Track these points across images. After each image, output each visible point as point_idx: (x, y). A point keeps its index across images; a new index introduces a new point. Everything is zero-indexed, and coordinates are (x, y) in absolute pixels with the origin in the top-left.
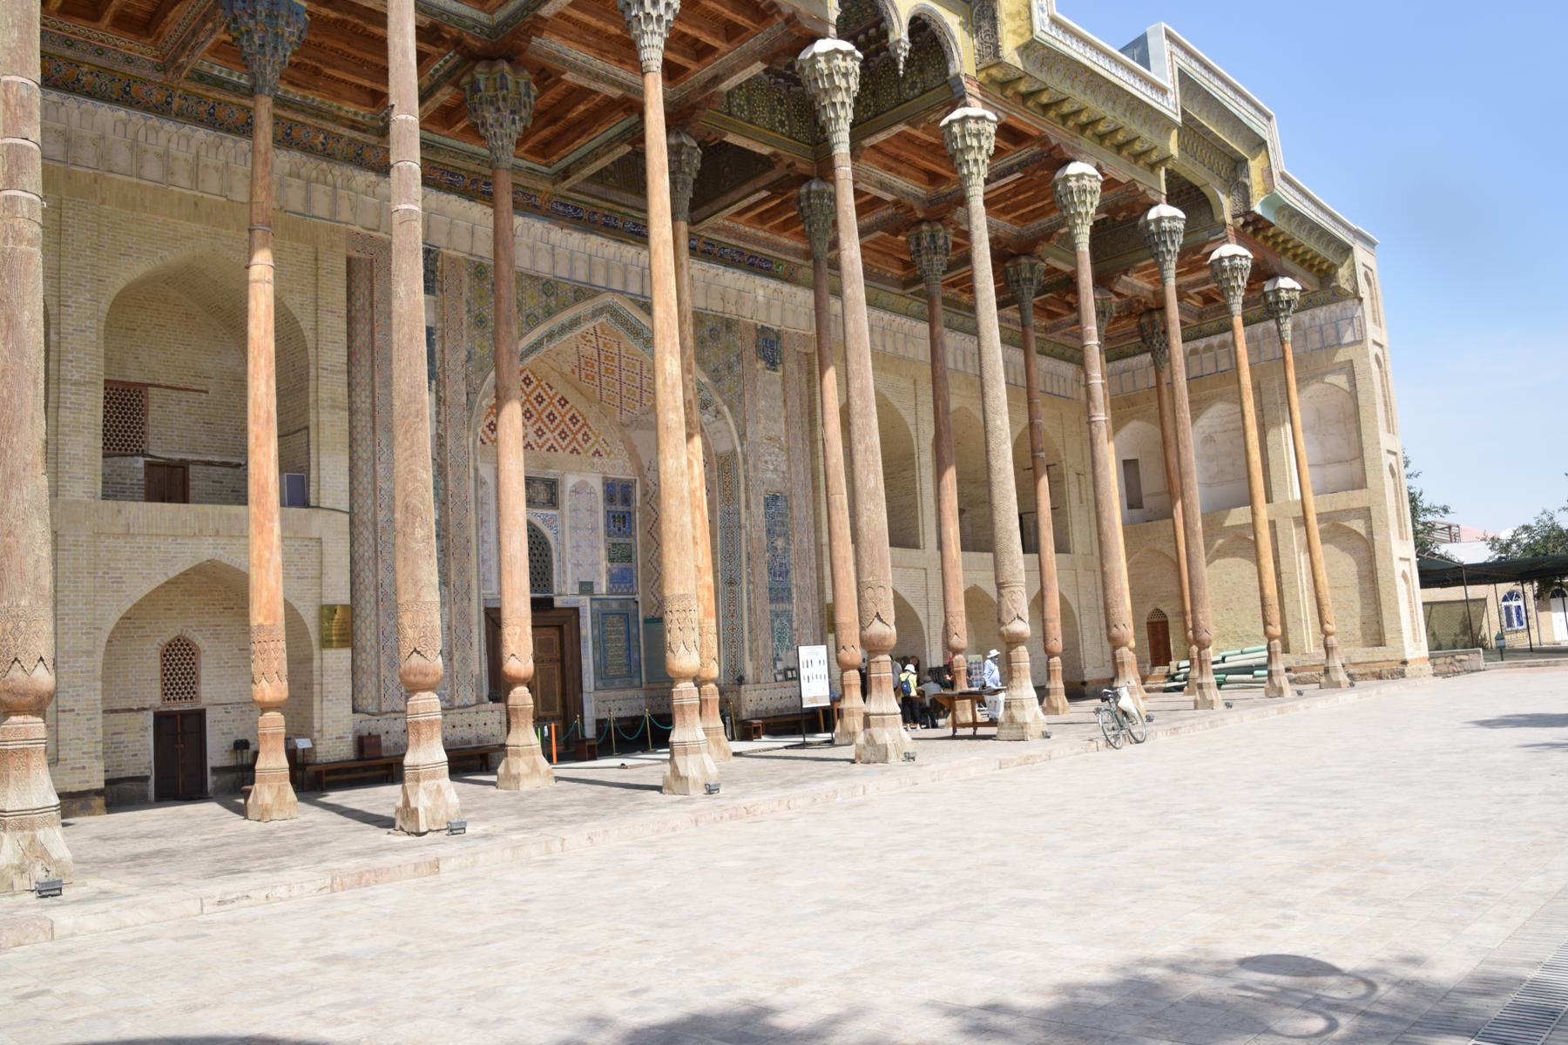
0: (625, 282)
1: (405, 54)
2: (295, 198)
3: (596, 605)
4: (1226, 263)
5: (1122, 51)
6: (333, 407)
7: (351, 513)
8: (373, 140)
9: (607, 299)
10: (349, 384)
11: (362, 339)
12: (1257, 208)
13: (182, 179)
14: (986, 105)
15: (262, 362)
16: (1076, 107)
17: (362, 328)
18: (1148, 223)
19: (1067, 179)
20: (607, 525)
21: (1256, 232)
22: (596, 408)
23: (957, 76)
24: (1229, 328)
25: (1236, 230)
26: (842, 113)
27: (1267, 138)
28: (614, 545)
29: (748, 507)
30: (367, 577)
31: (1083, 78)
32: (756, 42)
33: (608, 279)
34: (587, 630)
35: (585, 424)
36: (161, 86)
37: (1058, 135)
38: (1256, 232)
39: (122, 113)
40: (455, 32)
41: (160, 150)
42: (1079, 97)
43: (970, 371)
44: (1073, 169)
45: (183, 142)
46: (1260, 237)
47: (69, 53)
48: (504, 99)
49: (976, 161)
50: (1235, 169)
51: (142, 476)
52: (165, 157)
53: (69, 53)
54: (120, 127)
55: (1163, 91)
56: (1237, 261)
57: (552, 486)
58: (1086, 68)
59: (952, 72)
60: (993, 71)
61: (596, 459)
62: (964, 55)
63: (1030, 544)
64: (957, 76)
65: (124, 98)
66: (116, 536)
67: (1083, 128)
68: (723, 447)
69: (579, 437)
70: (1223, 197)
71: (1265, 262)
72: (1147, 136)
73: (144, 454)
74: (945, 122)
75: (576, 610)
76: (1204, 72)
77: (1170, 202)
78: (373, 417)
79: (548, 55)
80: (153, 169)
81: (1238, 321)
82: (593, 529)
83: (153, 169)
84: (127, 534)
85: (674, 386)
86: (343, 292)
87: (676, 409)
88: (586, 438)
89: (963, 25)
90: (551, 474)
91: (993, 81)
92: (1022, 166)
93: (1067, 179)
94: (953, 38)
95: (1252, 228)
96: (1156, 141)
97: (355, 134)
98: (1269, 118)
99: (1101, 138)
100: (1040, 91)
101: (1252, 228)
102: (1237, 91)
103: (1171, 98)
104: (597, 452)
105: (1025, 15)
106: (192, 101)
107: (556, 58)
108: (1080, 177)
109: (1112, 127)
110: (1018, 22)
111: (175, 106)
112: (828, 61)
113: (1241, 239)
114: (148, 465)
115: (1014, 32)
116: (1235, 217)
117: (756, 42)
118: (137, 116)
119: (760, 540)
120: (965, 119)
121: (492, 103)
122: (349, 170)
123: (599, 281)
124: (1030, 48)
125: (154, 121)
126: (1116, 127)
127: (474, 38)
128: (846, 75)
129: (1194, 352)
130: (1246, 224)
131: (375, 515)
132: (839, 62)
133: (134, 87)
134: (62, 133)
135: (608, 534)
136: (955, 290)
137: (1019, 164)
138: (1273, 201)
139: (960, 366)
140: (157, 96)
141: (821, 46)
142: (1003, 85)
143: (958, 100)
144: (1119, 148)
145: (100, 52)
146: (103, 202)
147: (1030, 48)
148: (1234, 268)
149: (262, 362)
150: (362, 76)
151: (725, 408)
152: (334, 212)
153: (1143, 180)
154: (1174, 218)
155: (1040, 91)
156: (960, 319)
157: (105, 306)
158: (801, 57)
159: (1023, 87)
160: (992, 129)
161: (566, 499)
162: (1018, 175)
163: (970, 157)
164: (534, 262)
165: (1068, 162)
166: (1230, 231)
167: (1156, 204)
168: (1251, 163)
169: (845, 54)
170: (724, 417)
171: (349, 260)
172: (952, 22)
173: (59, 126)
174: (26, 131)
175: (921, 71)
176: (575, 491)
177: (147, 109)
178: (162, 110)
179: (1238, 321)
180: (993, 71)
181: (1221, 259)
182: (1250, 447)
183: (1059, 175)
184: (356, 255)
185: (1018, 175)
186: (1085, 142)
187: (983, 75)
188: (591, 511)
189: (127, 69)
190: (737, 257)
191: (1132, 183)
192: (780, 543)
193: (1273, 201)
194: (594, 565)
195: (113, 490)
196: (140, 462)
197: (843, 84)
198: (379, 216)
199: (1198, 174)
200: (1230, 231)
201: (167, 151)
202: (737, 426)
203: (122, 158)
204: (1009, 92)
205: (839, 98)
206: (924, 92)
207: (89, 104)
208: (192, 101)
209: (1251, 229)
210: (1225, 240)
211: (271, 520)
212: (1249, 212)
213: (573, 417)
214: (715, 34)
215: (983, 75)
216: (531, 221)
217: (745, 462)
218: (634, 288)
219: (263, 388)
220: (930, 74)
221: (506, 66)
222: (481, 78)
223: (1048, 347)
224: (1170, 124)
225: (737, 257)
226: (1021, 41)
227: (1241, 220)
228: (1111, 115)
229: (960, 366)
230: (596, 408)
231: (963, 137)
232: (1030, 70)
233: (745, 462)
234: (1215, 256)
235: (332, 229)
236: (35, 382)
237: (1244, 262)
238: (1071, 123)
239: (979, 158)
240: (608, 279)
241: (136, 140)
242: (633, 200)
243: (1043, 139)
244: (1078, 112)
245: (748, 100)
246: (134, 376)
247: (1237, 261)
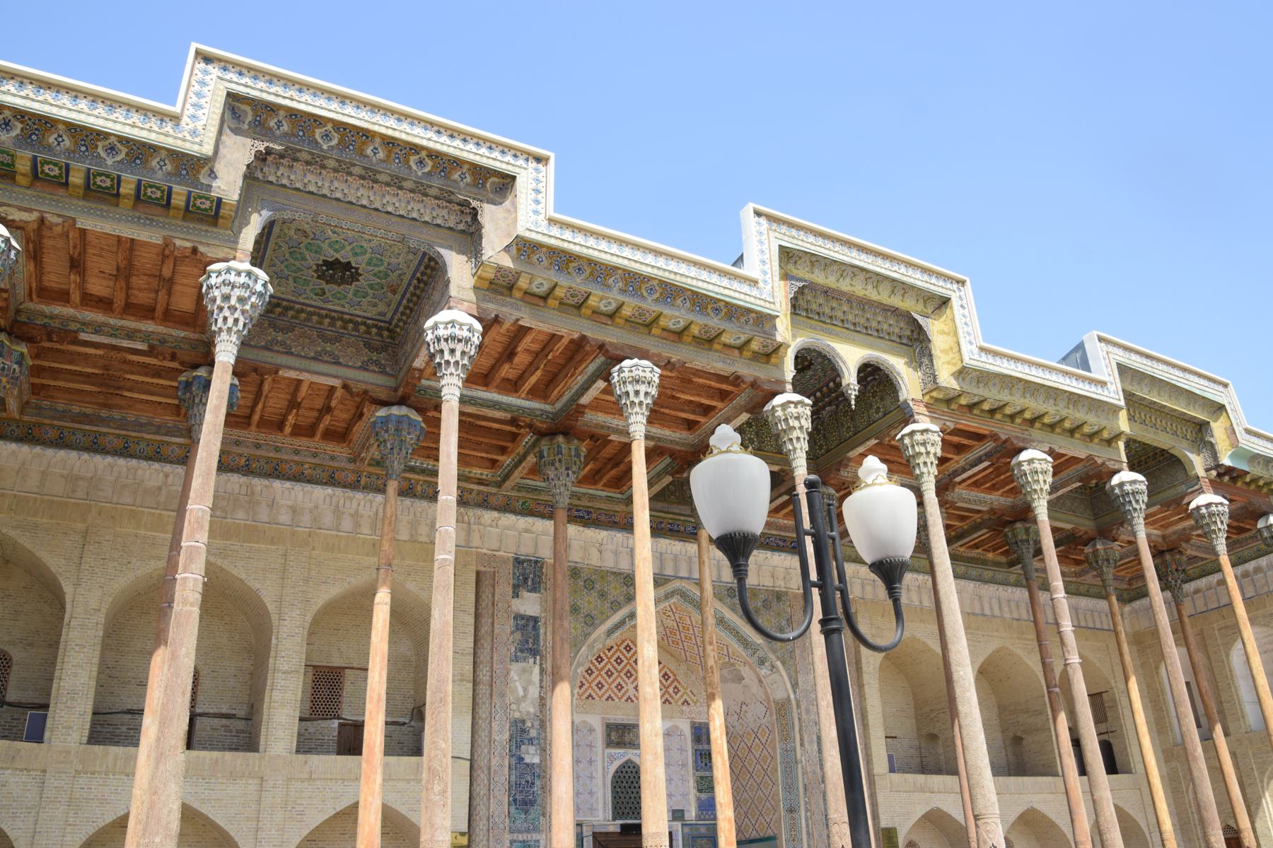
0: (690, 570)
1: (448, 456)
3: (687, 830)
4: (1204, 511)
5: (1064, 360)
6: (461, 680)
7: (472, 760)
8: (494, 490)
9: (676, 584)
10: (475, 663)
11: (485, 629)
12: (1226, 461)
13: (366, 529)
14: (933, 419)
15: (378, 659)
16: (1019, 408)
17: (486, 621)
18: (1113, 488)
19: (1020, 464)
20: (695, 761)
21: (1234, 479)
22: (684, 667)
23: (905, 401)
24: (1218, 569)
25: (1211, 481)
26: (798, 446)
27: (1225, 402)
28: (702, 778)
29: (802, 745)
30: (481, 810)
31: (1020, 386)
32: (741, 400)
33: (676, 569)
35: (675, 679)
36: (353, 471)
37: (1006, 431)
38: (1234, 479)
39: (329, 490)
40: (528, 420)
41: (352, 511)
42: (1017, 401)
43: (1007, 615)
44: (1024, 456)
45: (368, 505)
46: (1239, 484)
47: (296, 458)
48: (560, 461)
49: (925, 463)
50: (1200, 430)
51: (336, 734)
52: (356, 516)
53: (296, 458)
54: (328, 500)
55: (1103, 384)
56: (1214, 508)
58: (1020, 380)
59: (901, 399)
60: (934, 394)
61: (685, 708)
62: (910, 384)
63: (1083, 770)
64: (905, 401)
65: (331, 481)
66: (303, 781)
67: (1032, 422)
68: (779, 695)
69: (671, 690)
70: (1193, 457)
71: (1250, 503)
72: (1093, 421)
73: (339, 718)
74: (899, 437)
76: (1145, 361)
77: (1132, 468)
78: (491, 686)
79: (597, 425)
80: (347, 524)
81: (1225, 560)
82: (683, 765)
83: (347, 524)
84: (310, 779)
85: (650, 667)
86: (473, 596)
87: (652, 684)
88: (677, 691)
89: (909, 364)
91: (937, 400)
92: (988, 456)
93: (1020, 464)
94: (899, 374)
95: (1226, 478)
96: (1104, 423)
97: (482, 488)
98: (1226, 386)
99: (1052, 427)
100: (982, 402)
101: (1226, 478)
102: (1184, 370)
103: (1112, 388)
104: (686, 701)
105: (956, 349)
106: (374, 478)
107: (603, 427)
108: (1031, 461)
109: (1058, 418)
110: (952, 355)
111: (362, 483)
112: (784, 410)
113: (1217, 486)
114: (341, 725)
115: (949, 363)
116: (1207, 470)
117: (741, 400)
118: (339, 491)
119: (814, 772)
120: (912, 433)
121: (553, 464)
122: (479, 512)
123: (669, 571)
124: (962, 373)
125: (349, 493)
126: (1061, 418)
127: (542, 422)
128: (797, 418)
129: (1246, 575)
130: (1219, 475)
131: (489, 761)
132: (792, 409)
133: (337, 474)
134: (291, 507)
135: (696, 768)
136: (979, 551)
137: (986, 455)
138: (1238, 453)
139: (997, 612)
140: (351, 478)
141: (778, 400)
142: (948, 401)
143: (908, 418)
144: (1072, 432)
145: (315, 455)
146: (314, 549)
147: (962, 373)
148: (1211, 515)
149: (378, 659)
150: (482, 451)
151: (779, 663)
152: (468, 540)
153: (1101, 454)
154: (1134, 482)
155: (982, 402)
156: (990, 574)
157: (309, 618)
158: (765, 409)
159: (963, 401)
160: (937, 439)
162: (986, 464)
163: (920, 460)
164: (616, 562)
165: (1020, 450)
166: (1205, 484)
167: (1118, 471)
168: (1212, 424)
169: (796, 404)
170: (778, 671)
171: (478, 573)
172: (897, 364)
173: (290, 503)
174: (198, 537)
175: (882, 399)
177: (344, 487)
178: (354, 486)
179: (1225, 560)
180: (934, 394)
181: (1198, 508)
182: (1255, 672)
183: (1014, 462)
184: (483, 569)
185: (986, 464)
186: (1036, 433)
187: (927, 397)
188: (682, 750)
189: (331, 464)
190: (781, 544)
191: (1090, 458)
193: (1238, 453)
194: (684, 795)
195: (306, 745)
196: (336, 723)
197: (796, 424)
198: (500, 541)
199: (1161, 439)
200: (1205, 484)
201: (357, 512)
202: (790, 678)
203: (328, 520)
204: (954, 406)
205: (795, 434)
206: (885, 415)
207: (309, 487)
208: (374, 478)
209: (1226, 478)
210: (1201, 491)
211: (375, 773)
212: (1218, 466)
213: (666, 674)
214: (712, 398)
215: (927, 397)
216: (613, 533)
217: (798, 706)
218: (696, 576)
219: (377, 678)
220: (888, 401)
221: (561, 439)
222: (545, 448)
223: (1082, 589)
224: (1115, 409)
225: (781, 544)
226: (955, 369)
227: (1214, 473)
228: (1052, 411)
229: (997, 612)
230: (684, 667)
231: (913, 446)
232: (967, 388)
233: (798, 706)
234: (1193, 505)
235: (467, 553)
236: (183, 693)
237: (1220, 508)
238: (1018, 420)
239: (928, 461)
240: (676, 569)
241: (337, 506)
242: (685, 509)
243: (994, 437)
244: (1022, 412)
245: (757, 434)
246: (337, 662)
247: (1214, 508)
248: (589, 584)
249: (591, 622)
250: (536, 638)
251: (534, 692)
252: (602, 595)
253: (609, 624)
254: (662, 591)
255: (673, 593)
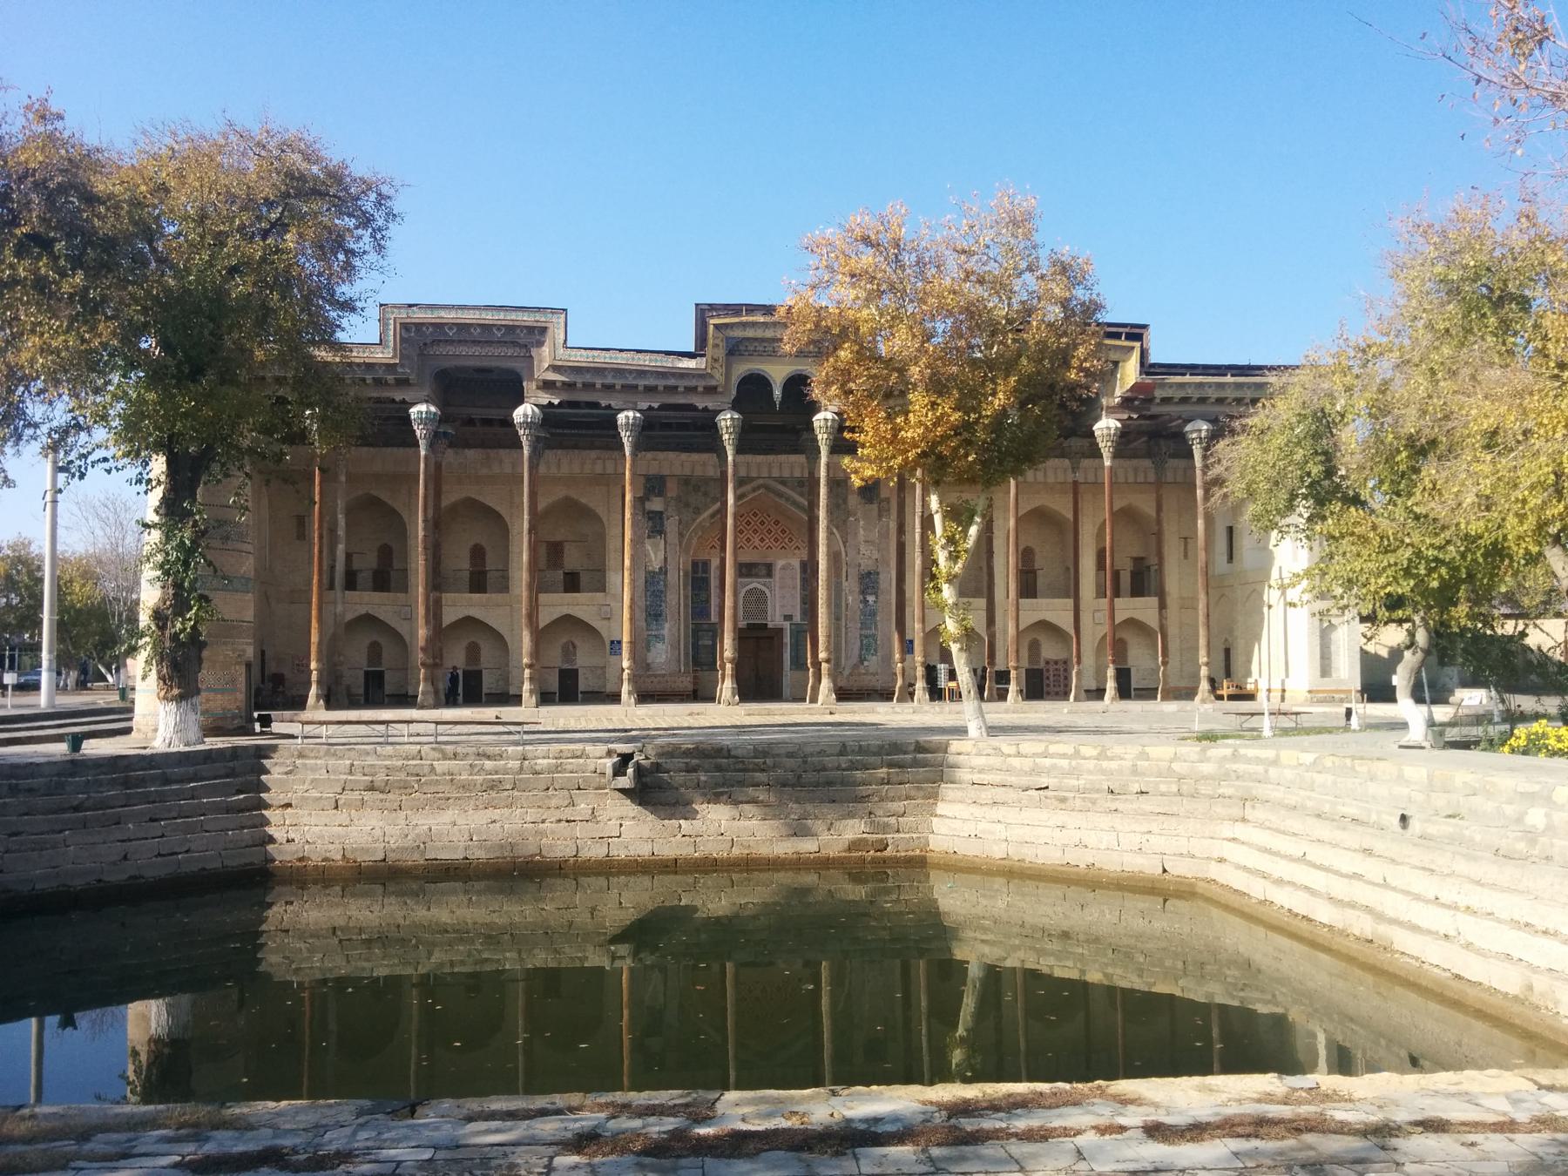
2: (598, 469)
9: (761, 481)
34: (787, 639)
57: (769, 570)
75: (780, 631)
90: (768, 560)
143: (818, 411)
161: (777, 573)
176: (783, 568)
192: (871, 599)
218: (775, 474)
246: (558, 538)
248: (697, 489)
249: (698, 511)
250: (662, 525)
251: (661, 555)
252: (706, 494)
253: (710, 511)
254: (748, 488)
255: (759, 488)
